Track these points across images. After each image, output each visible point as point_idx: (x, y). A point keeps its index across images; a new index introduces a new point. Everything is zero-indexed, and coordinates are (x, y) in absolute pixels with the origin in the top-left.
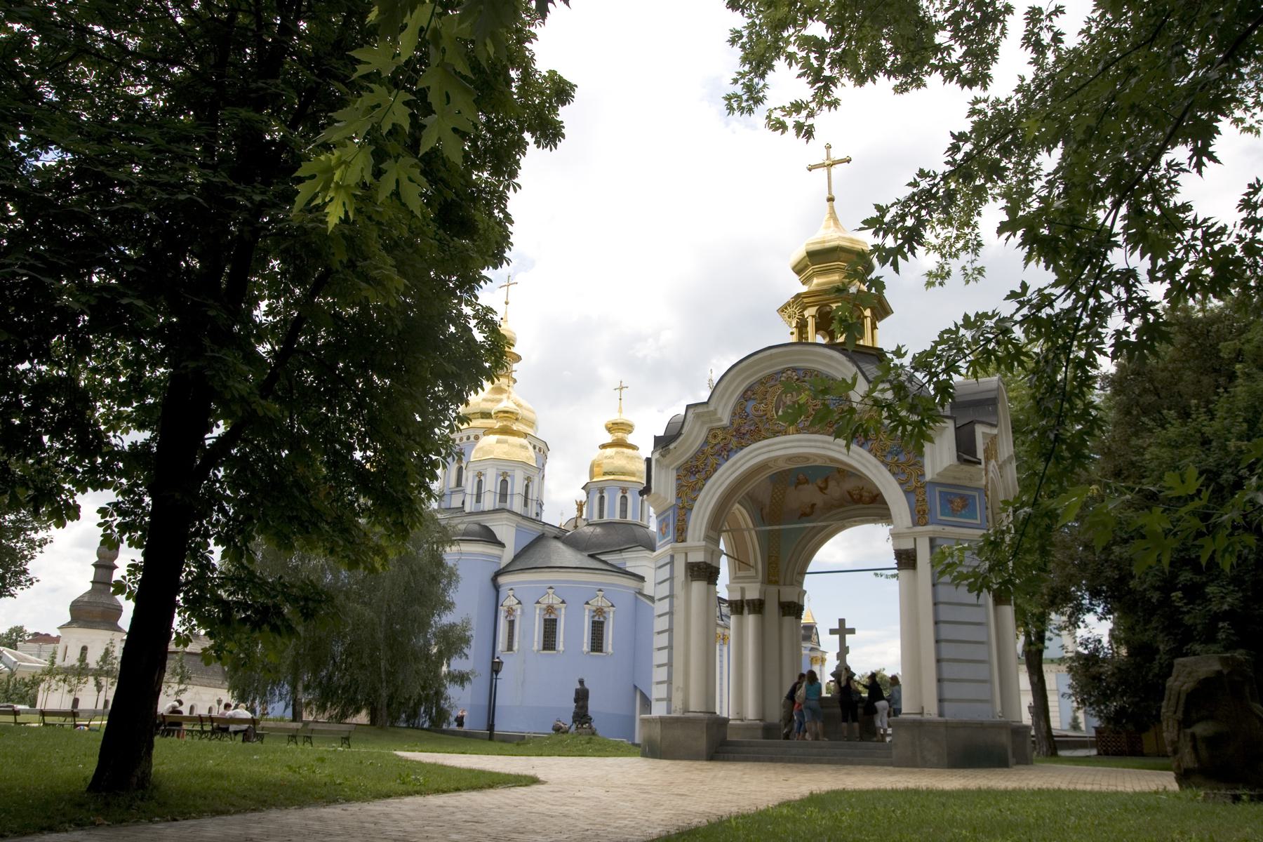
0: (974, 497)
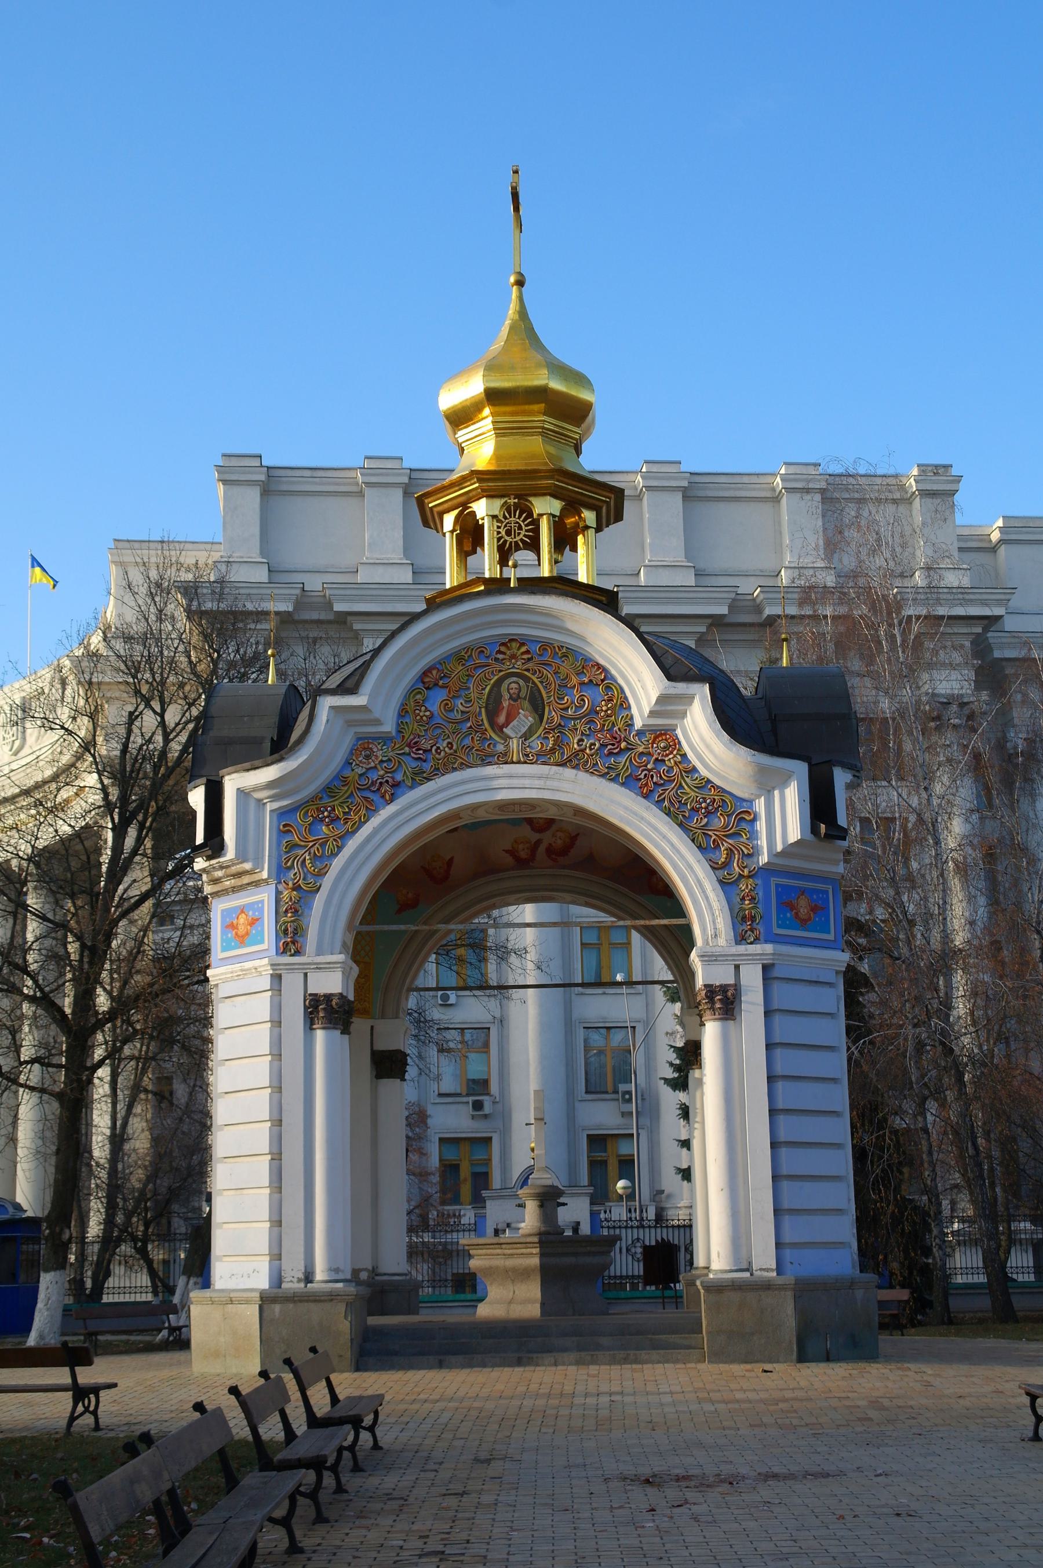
0: (827, 892)
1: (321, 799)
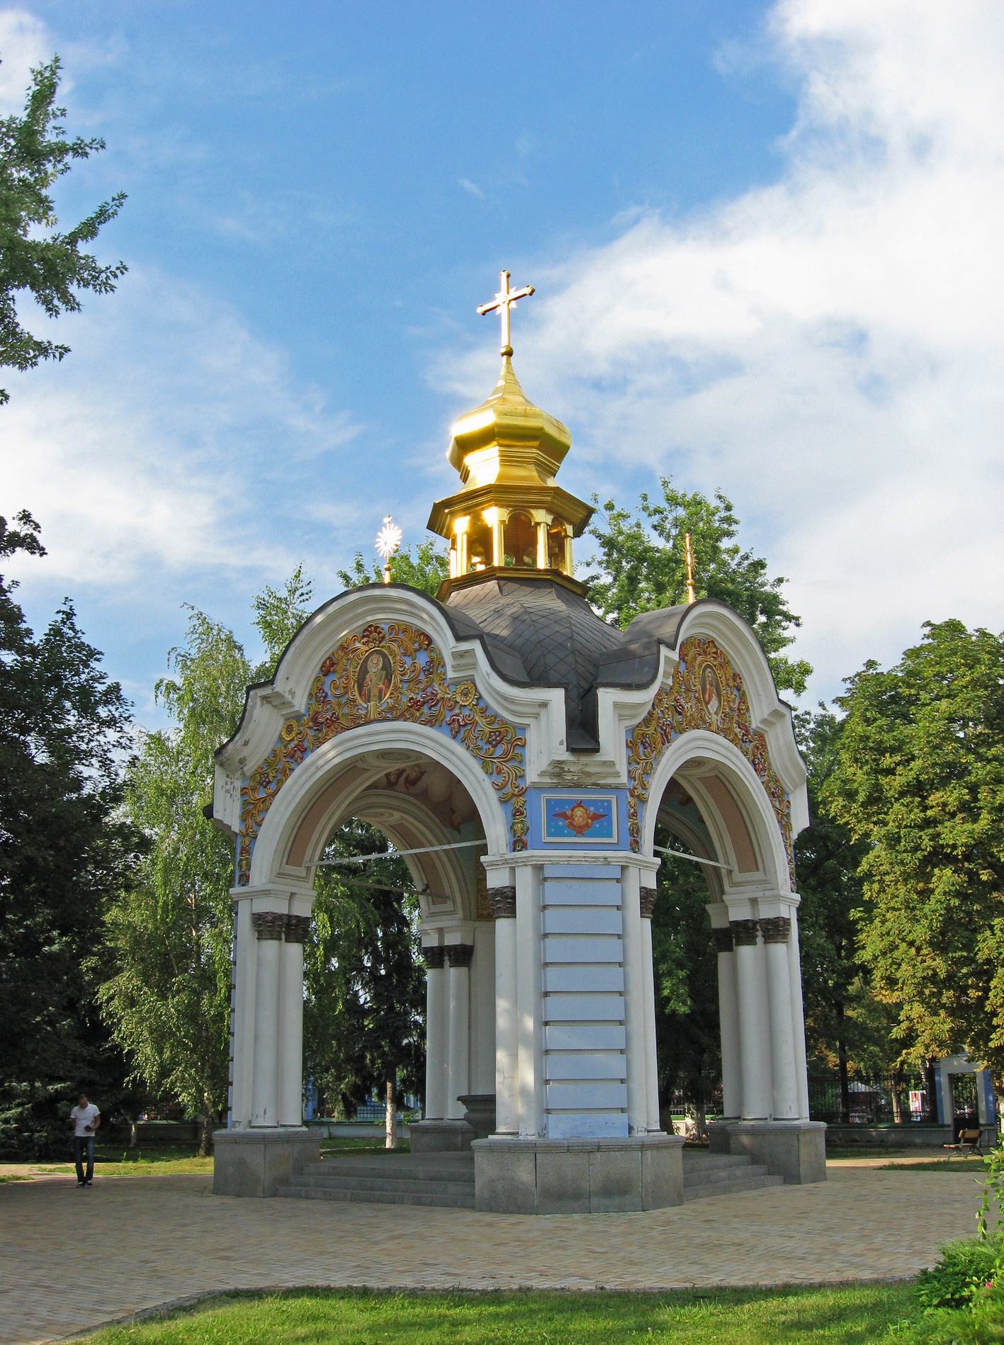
0: (609, 802)
1: (262, 768)
